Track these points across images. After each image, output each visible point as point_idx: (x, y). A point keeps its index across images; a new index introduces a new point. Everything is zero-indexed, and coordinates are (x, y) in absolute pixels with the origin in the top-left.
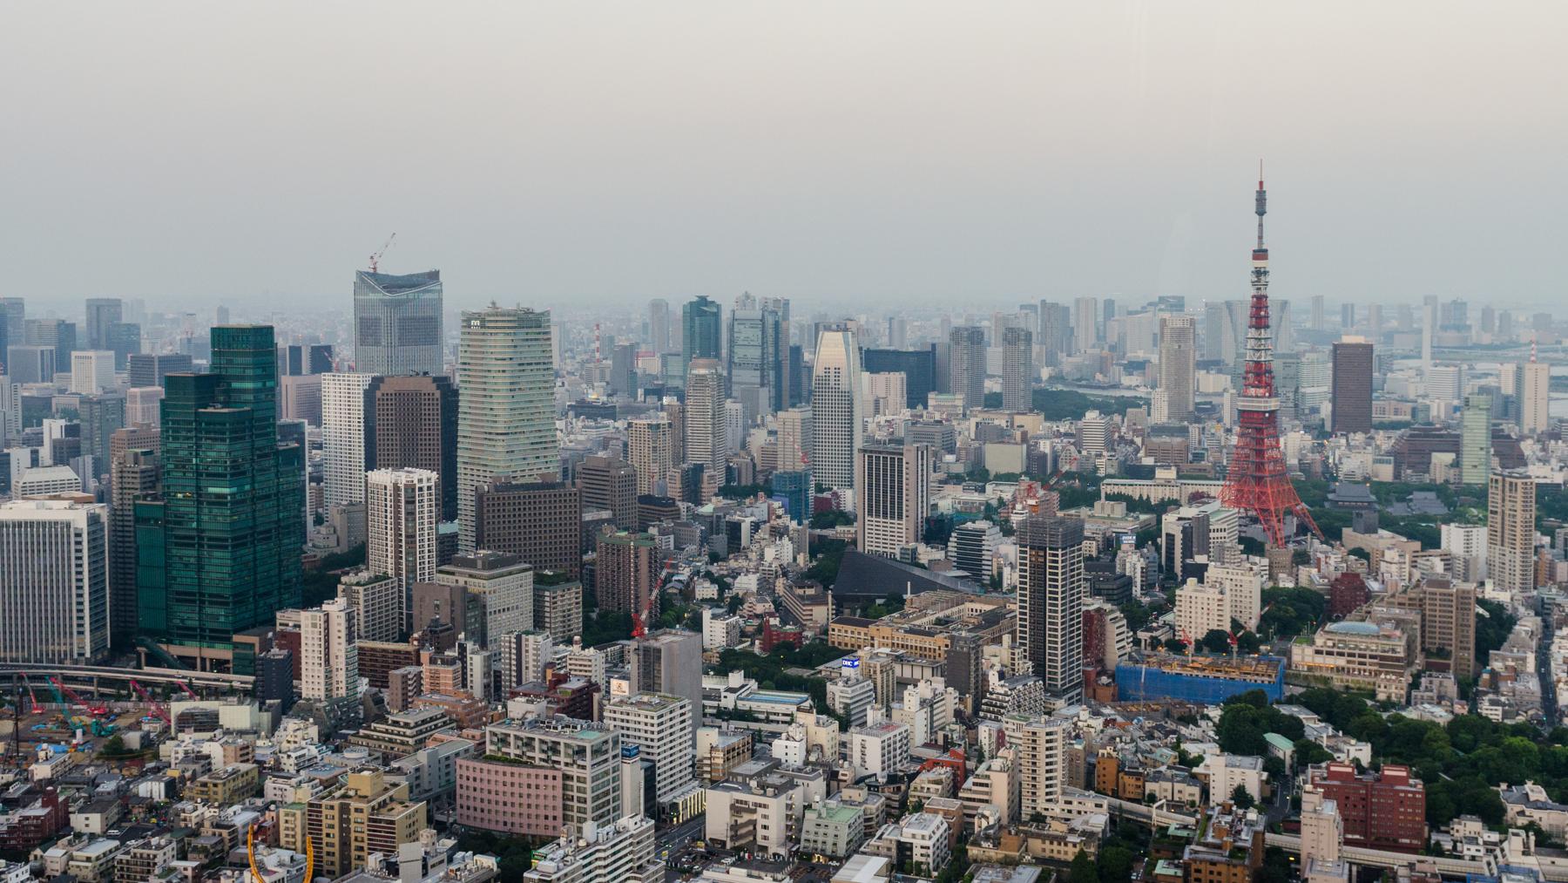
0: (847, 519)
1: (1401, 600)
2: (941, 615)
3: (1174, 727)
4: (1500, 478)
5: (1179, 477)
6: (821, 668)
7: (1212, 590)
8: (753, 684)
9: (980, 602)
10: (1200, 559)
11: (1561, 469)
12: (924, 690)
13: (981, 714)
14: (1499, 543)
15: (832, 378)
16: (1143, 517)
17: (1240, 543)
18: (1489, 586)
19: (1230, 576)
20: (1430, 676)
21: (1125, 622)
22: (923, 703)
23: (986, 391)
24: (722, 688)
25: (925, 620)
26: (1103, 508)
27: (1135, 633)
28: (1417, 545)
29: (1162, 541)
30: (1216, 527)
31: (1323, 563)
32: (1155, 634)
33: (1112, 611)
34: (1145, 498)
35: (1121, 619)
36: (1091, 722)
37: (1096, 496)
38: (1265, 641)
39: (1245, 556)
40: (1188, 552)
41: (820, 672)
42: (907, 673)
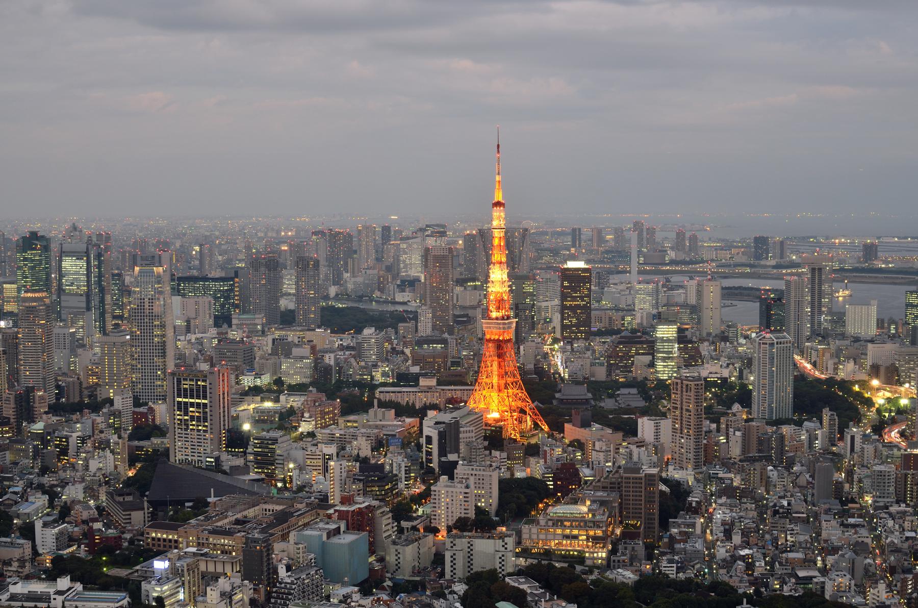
0: (160, 431)
1: (605, 485)
2: (239, 516)
3: (428, 601)
4: (679, 381)
5: (439, 383)
6: (138, 567)
7: (459, 485)
8: (79, 587)
9: (273, 503)
10: (452, 457)
11: (728, 365)
12: (223, 584)
13: (273, 600)
14: (679, 431)
15: (147, 306)
16: (408, 420)
17: (485, 438)
18: (671, 468)
19: (474, 472)
20: (625, 543)
21: (390, 515)
22: (223, 594)
23: (283, 309)
24: (52, 591)
25: (226, 521)
26: (375, 415)
27: (399, 523)
28: (620, 435)
29: (423, 441)
30: (465, 429)
31: (548, 455)
32: (415, 523)
33: (380, 507)
34: (410, 404)
35: (387, 514)
36: (362, 602)
37: (372, 406)
38: (502, 523)
39: (487, 452)
40: (442, 452)
41: (137, 571)
42: (211, 568)
